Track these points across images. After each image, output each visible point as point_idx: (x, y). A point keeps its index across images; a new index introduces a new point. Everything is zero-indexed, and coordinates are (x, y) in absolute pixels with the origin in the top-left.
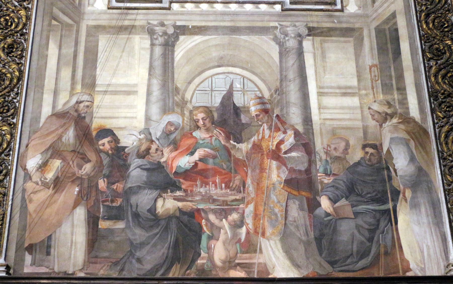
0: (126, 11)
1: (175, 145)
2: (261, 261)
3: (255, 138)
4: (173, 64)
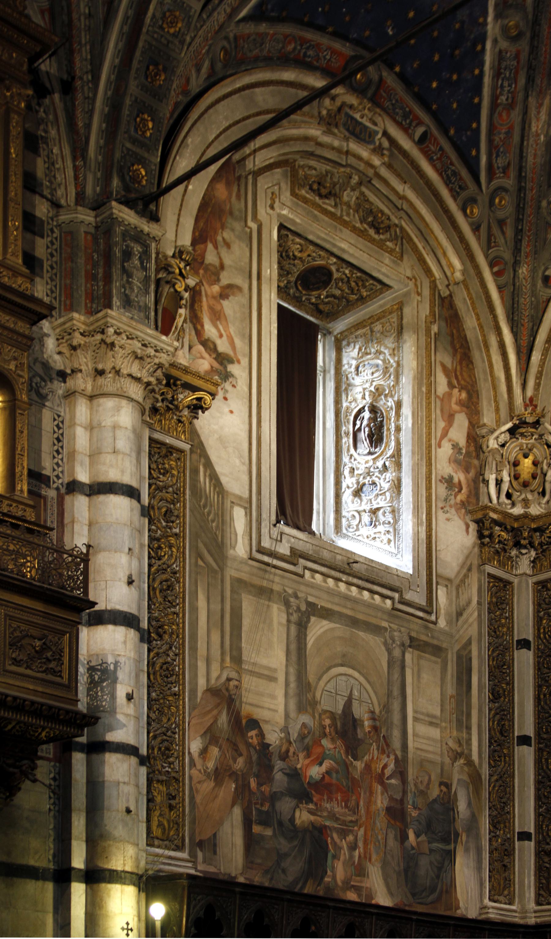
1: (308, 753)
2: (368, 885)
3: (366, 758)
4: (305, 652)
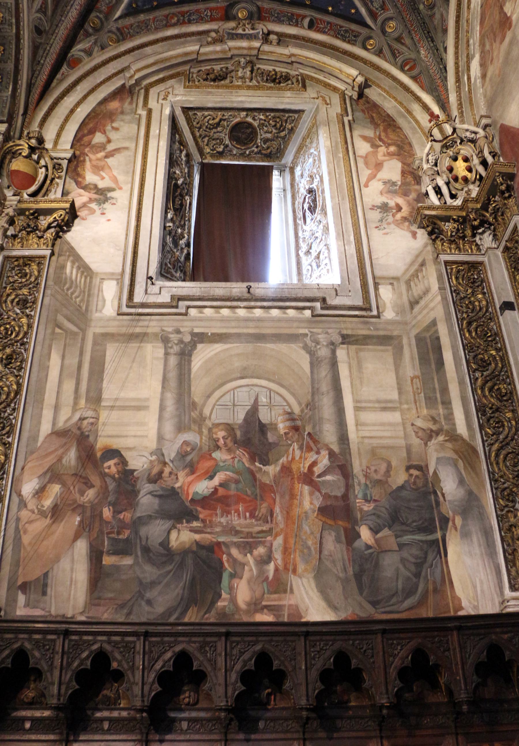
0: (137, 317)
1: (192, 468)
2: (292, 602)
3: (283, 460)
4: (190, 374)
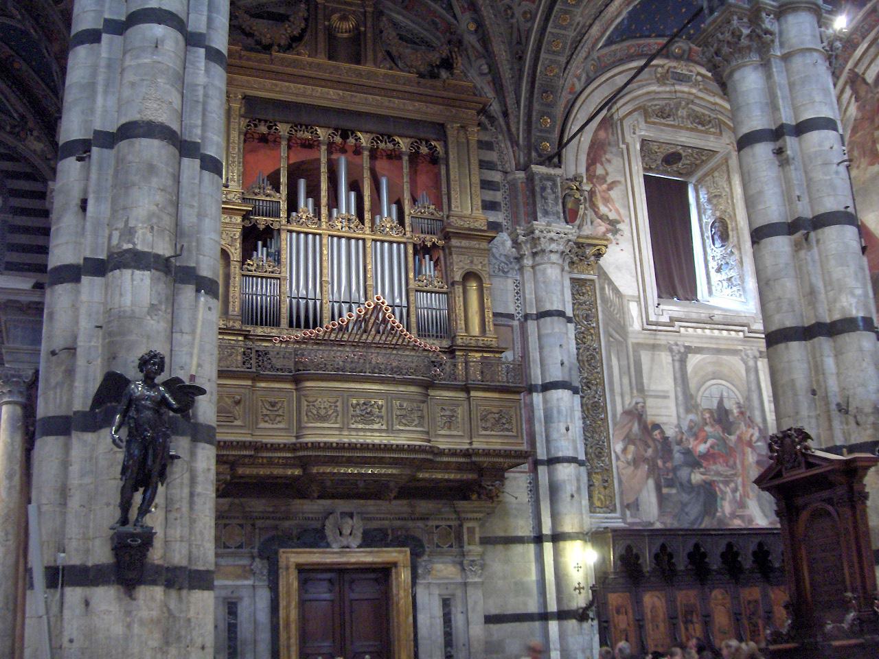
1: (696, 436)
3: (738, 432)
